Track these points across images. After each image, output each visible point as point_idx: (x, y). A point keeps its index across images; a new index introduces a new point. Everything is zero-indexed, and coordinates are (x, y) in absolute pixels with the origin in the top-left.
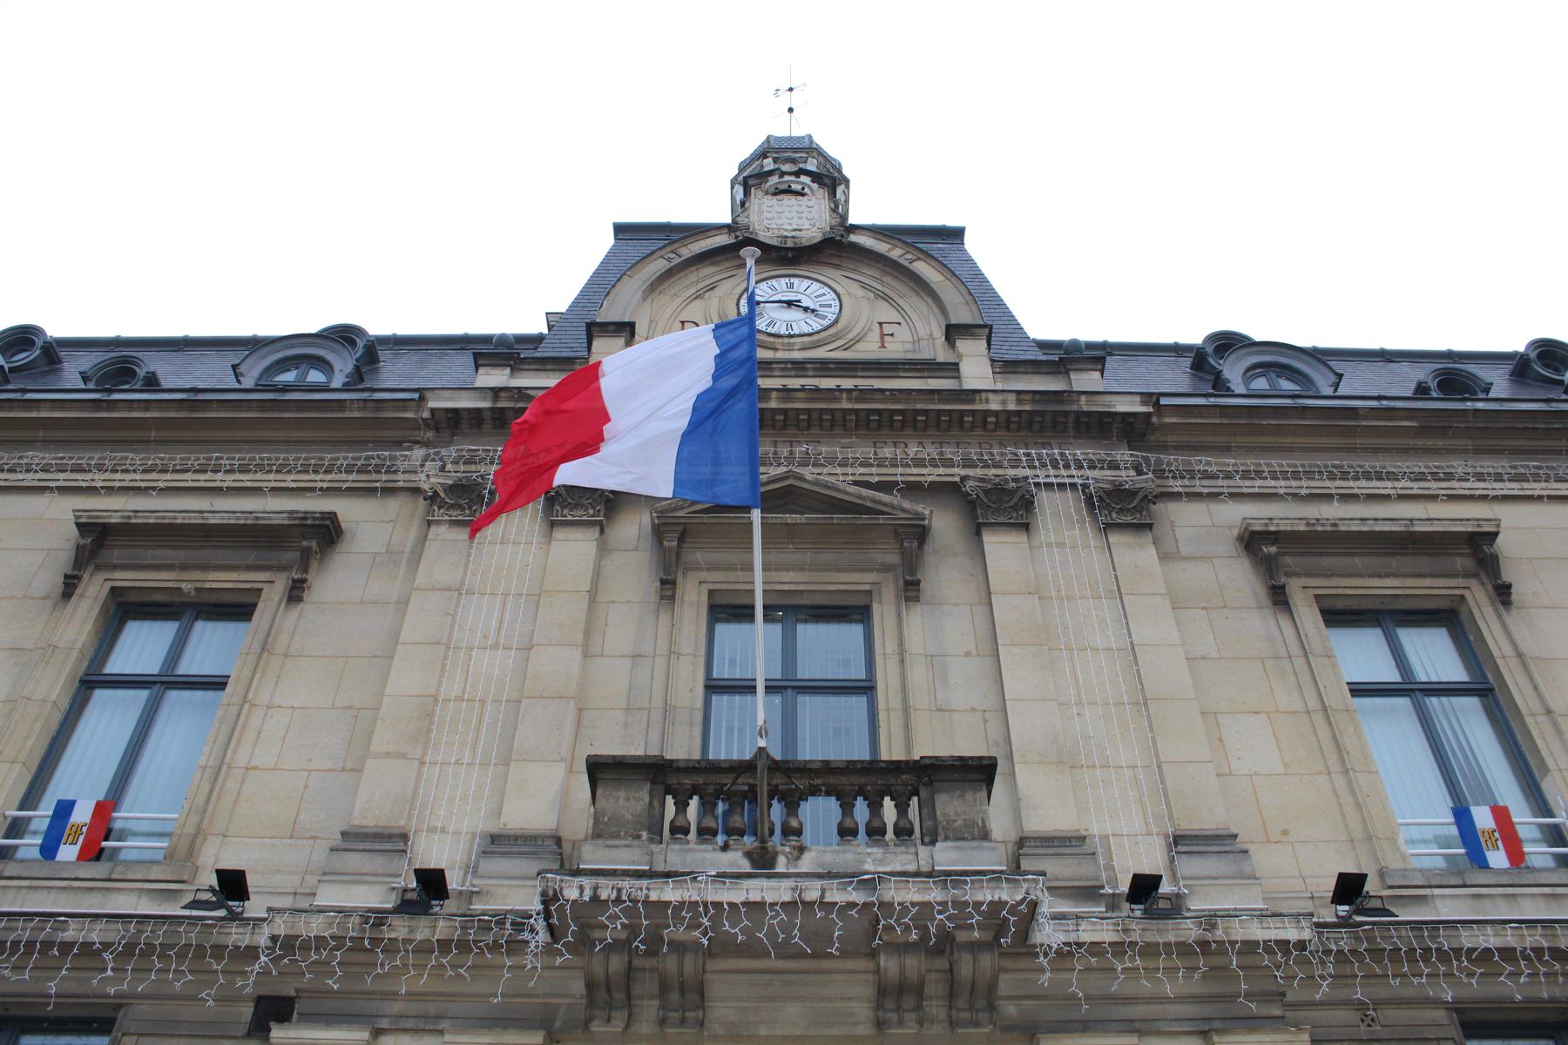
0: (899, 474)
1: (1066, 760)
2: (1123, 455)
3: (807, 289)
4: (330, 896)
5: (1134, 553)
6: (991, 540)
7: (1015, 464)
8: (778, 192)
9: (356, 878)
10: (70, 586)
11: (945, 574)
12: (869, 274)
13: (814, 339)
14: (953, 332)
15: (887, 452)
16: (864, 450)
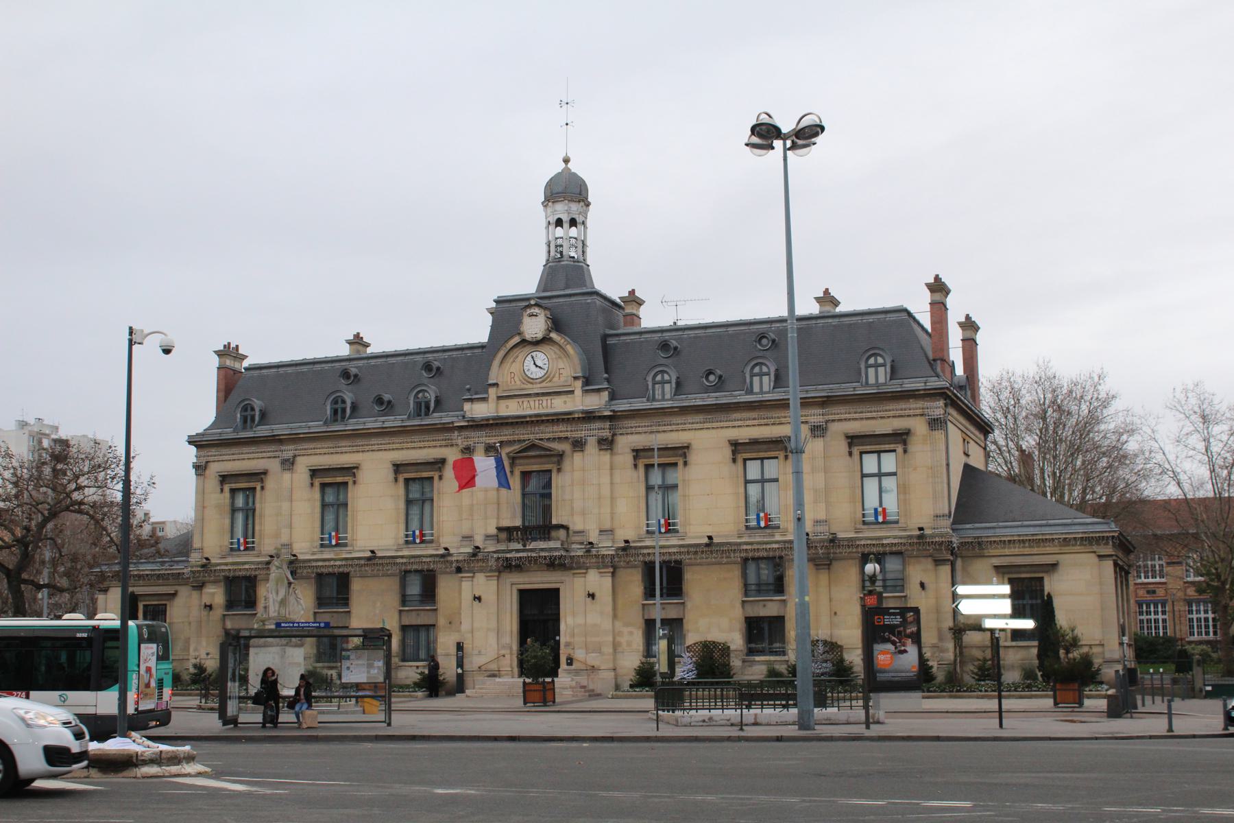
0: (556, 435)
1: (583, 513)
2: (607, 424)
3: (541, 358)
4: (462, 550)
5: (606, 457)
6: (575, 454)
7: (580, 432)
8: (531, 315)
9: (465, 546)
10: (396, 480)
11: (566, 464)
12: (555, 348)
13: (542, 380)
14: (576, 378)
15: (555, 428)
16: (550, 429)
